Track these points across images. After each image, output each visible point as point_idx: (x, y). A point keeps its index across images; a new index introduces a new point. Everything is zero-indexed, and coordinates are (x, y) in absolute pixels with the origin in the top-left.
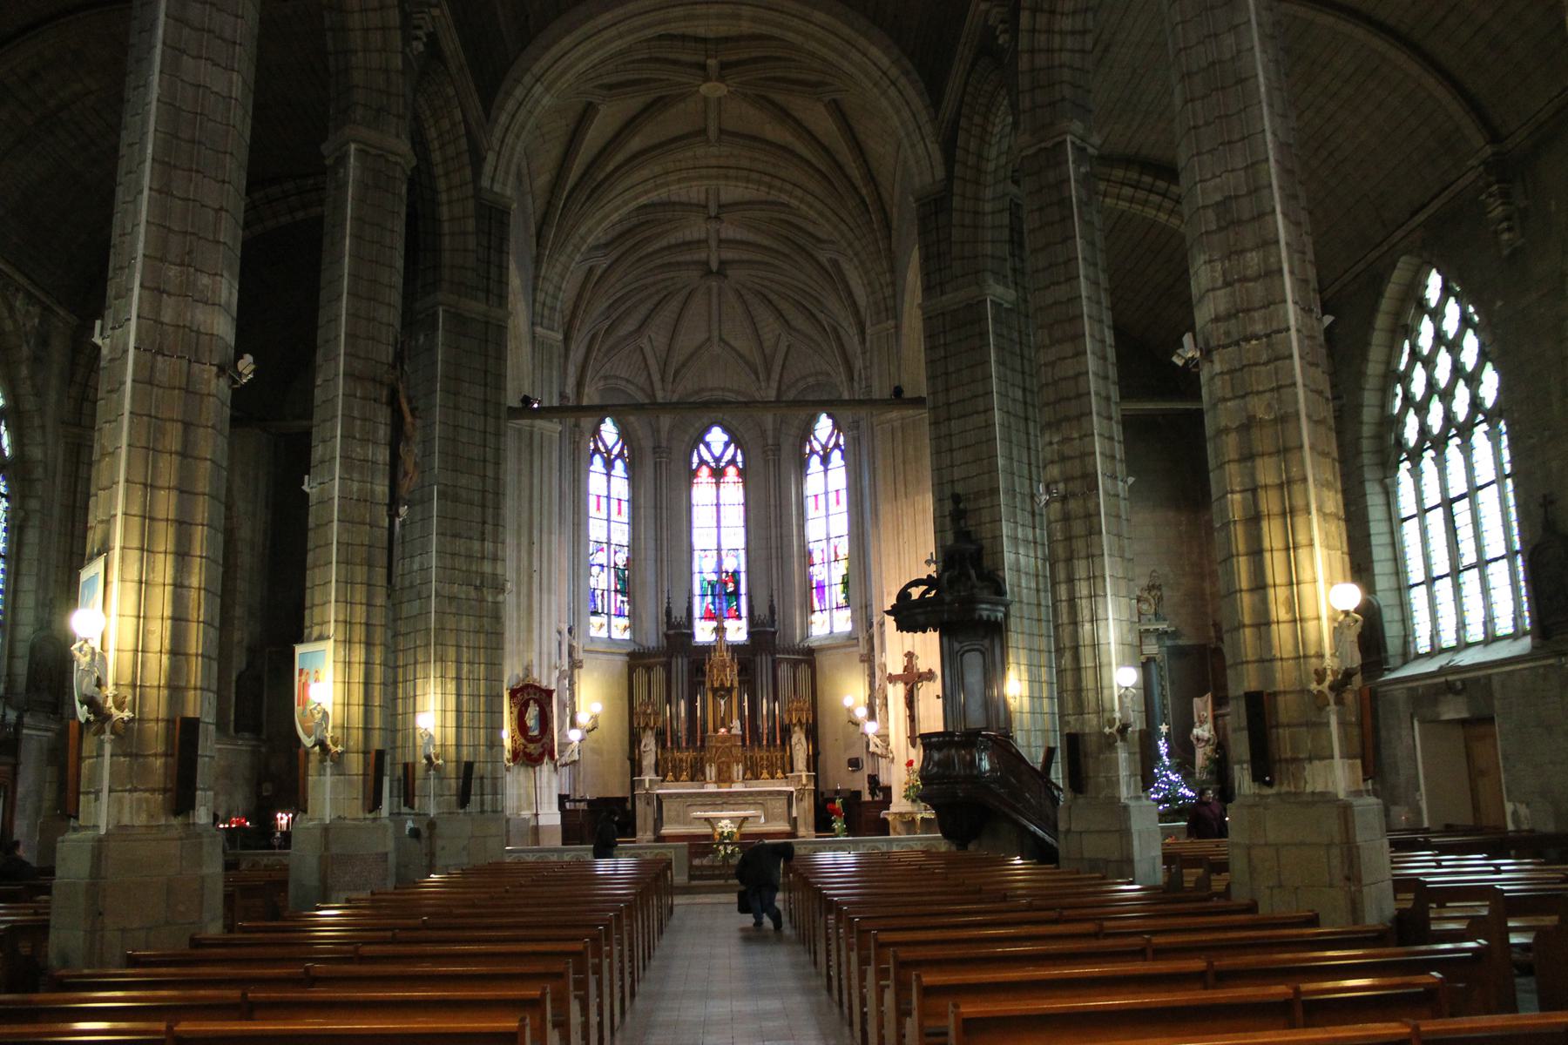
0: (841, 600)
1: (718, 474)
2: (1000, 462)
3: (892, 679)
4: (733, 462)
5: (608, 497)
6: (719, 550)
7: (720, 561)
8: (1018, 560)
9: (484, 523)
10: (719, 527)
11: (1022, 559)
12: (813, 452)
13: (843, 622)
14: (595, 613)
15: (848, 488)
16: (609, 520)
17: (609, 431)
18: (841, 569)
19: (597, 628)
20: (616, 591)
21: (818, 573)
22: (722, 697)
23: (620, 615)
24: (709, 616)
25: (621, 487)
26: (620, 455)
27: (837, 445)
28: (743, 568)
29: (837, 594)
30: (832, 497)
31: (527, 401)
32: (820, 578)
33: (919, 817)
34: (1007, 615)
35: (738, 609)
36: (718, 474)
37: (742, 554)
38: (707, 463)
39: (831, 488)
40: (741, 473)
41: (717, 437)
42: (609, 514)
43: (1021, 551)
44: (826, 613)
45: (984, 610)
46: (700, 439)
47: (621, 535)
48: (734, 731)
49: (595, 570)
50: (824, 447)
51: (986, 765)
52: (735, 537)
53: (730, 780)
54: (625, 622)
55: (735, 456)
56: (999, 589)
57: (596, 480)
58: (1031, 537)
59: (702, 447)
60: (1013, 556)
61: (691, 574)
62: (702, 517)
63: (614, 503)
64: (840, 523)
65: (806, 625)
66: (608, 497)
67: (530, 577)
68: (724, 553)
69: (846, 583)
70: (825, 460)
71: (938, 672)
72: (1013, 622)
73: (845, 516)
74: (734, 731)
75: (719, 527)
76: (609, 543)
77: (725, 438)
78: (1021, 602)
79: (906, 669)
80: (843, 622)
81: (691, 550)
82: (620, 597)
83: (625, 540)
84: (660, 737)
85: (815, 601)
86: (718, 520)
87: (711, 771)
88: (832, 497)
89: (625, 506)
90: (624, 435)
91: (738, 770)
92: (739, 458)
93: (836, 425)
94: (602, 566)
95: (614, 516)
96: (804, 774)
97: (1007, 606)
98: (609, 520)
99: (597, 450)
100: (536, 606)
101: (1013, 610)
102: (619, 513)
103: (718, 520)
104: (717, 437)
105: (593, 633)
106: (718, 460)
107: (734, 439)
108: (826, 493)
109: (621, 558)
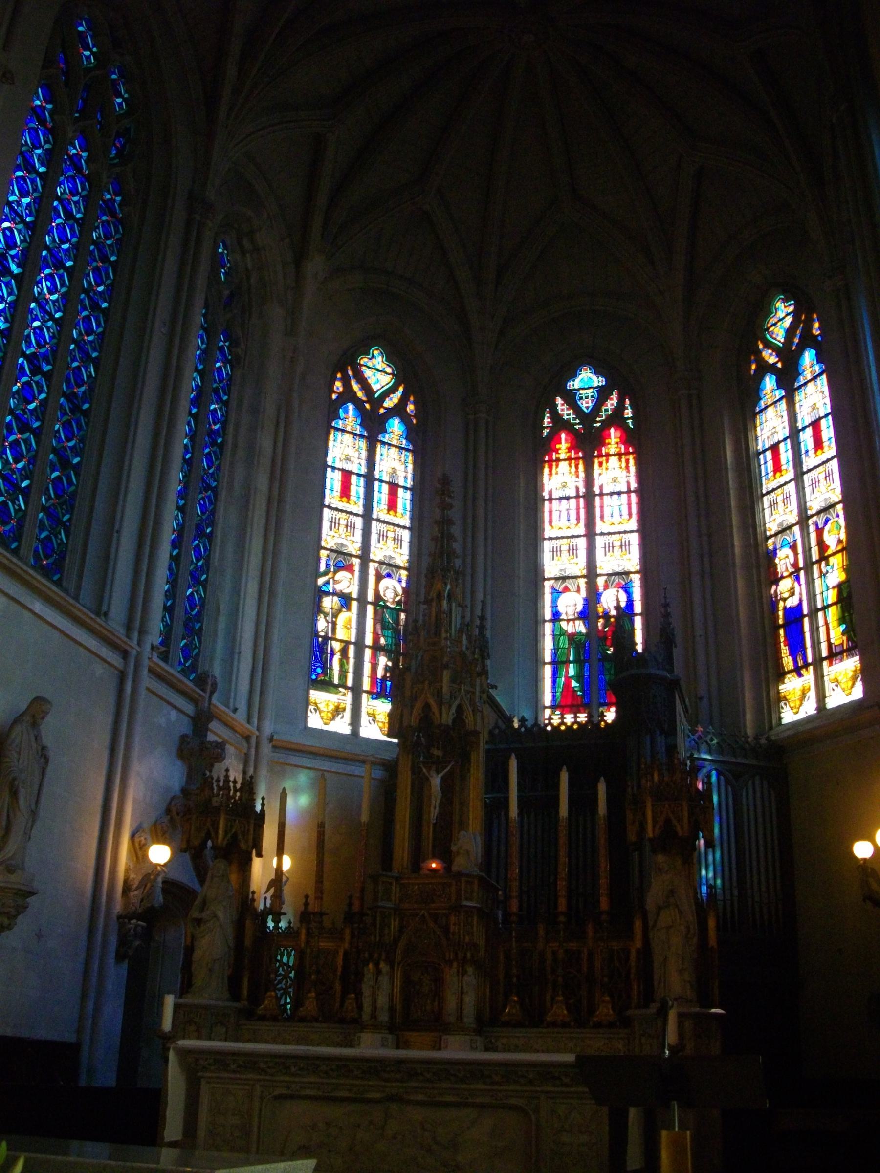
0: (837, 634)
1: (589, 446)
4: (616, 418)
5: (370, 479)
6: (591, 574)
7: (593, 597)
10: (590, 534)
12: (765, 368)
14: (326, 685)
15: (836, 413)
16: (367, 516)
17: (378, 372)
19: (325, 713)
20: (376, 648)
21: (789, 592)
22: (439, 765)
25: (395, 463)
26: (398, 411)
28: (638, 608)
30: (807, 437)
32: (792, 602)
36: (589, 446)
37: (636, 579)
38: (567, 426)
39: (804, 417)
41: (586, 381)
44: (809, 675)
46: (557, 384)
47: (394, 547)
48: (460, 864)
49: (328, 603)
52: (623, 555)
53: (438, 1026)
54: (383, 707)
57: (344, 449)
59: (559, 401)
61: (537, 622)
62: (560, 521)
63: (381, 494)
64: (826, 488)
65: (772, 702)
66: (370, 479)
68: (601, 581)
69: (846, 596)
70: (789, 380)
73: (834, 465)
74: (460, 864)
75: (590, 534)
76: (365, 556)
77: (598, 381)
81: (536, 577)
82: (383, 661)
83: (402, 557)
85: (785, 650)
86: (590, 531)
87: (381, 990)
88: (807, 437)
89: (404, 498)
90: (404, 375)
91: (463, 991)
92: (628, 413)
94: (346, 599)
95: (380, 509)
98: (367, 516)
99: (348, 395)
102: (392, 505)
103: (590, 531)
104: (586, 381)
105: (314, 721)
106: (587, 418)
107: (616, 379)
108: (794, 434)
109: (392, 589)
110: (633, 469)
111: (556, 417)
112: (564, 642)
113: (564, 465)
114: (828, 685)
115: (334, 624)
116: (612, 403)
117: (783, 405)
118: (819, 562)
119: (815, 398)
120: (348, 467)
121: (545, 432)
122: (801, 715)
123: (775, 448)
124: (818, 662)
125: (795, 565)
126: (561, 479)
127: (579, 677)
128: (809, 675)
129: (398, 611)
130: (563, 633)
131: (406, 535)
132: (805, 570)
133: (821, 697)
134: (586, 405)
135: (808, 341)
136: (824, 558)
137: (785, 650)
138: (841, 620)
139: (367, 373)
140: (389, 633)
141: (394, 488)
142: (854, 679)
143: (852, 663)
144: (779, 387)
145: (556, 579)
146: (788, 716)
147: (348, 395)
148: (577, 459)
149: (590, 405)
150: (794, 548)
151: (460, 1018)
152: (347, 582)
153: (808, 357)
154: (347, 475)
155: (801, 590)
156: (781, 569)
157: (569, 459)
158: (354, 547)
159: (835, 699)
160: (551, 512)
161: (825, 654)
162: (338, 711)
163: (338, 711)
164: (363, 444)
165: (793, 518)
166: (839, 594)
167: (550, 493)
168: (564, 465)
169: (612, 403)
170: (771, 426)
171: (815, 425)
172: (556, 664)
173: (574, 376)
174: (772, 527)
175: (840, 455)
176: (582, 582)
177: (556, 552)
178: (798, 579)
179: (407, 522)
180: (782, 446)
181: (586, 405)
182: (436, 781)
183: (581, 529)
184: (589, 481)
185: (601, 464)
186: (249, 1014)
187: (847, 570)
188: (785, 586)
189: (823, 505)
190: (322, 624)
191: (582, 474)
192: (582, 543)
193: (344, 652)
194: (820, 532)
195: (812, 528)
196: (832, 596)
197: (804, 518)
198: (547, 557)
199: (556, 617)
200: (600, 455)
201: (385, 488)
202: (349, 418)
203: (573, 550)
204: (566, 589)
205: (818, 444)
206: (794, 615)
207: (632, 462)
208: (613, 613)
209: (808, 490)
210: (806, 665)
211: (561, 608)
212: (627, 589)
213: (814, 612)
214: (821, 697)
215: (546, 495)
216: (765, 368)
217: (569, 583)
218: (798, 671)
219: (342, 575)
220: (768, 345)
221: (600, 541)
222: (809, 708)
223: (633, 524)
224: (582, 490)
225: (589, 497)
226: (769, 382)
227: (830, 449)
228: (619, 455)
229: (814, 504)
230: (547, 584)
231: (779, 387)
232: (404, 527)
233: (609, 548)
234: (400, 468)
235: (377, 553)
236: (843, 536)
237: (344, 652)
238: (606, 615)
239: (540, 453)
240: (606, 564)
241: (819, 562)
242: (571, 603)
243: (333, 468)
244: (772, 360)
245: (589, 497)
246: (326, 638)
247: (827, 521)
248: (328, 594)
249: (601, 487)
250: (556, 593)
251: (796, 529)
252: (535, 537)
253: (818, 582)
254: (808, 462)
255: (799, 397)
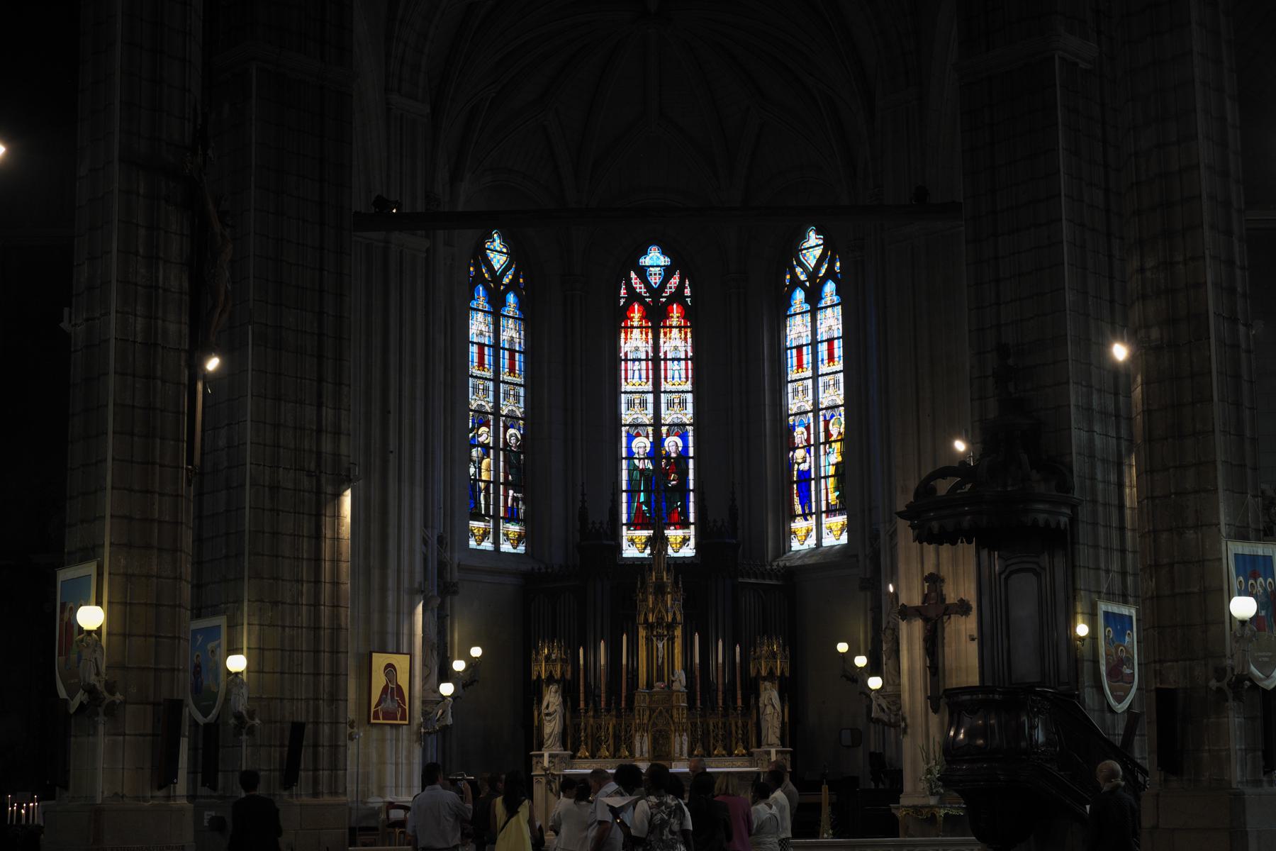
0: (833, 497)
2: (1069, 297)
3: (906, 613)
4: (678, 296)
6: (657, 422)
7: (658, 442)
8: (1091, 441)
9: (320, 380)
10: (657, 392)
11: (1098, 440)
12: (796, 283)
13: (835, 532)
14: (478, 517)
15: (845, 337)
16: (496, 380)
18: (835, 458)
22: (660, 637)
23: (512, 517)
24: (637, 522)
25: (511, 332)
26: (512, 286)
27: (830, 274)
29: (829, 492)
30: (823, 348)
31: (382, 204)
32: (804, 467)
33: (942, 812)
34: (1073, 520)
35: (685, 512)
39: (823, 334)
40: (687, 314)
41: (655, 259)
42: (497, 372)
43: (1097, 428)
44: (812, 521)
45: (1041, 514)
49: (475, 453)
50: (812, 275)
51: (1040, 736)
54: (514, 528)
55: (681, 287)
56: (1065, 486)
57: (478, 325)
58: (1111, 408)
59: (633, 275)
60: (1084, 435)
61: (617, 460)
62: (634, 379)
65: (785, 535)
66: (496, 347)
67: (385, 462)
68: (664, 430)
70: (814, 297)
71: (974, 605)
72: (1083, 531)
75: (657, 392)
77: (664, 261)
78: (1094, 502)
79: (926, 598)
80: (835, 532)
81: (617, 422)
82: (511, 492)
84: (569, 692)
85: (796, 500)
88: (823, 348)
92: (688, 292)
93: (827, 245)
94: (485, 447)
96: (773, 751)
97: (1074, 507)
98: (496, 380)
99: (479, 278)
100: (392, 502)
101: (1084, 513)
104: (655, 259)
105: (472, 543)
106: (656, 292)
108: (814, 343)
110: (689, 341)
111: (630, 289)
112: (636, 475)
113: (636, 332)
114: (825, 531)
115: (480, 469)
116: (675, 281)
117: (808, 317)
118: (825, 444)
119: (831, 322)
120: (482, 340)
121: (622, 301)
122: (805, 547)
123: (799, 348)
124: (819, 514)
125: (808, 440)
126: (634, 343)
127: (647, 503)
128: (812, 521)
129: (518, 454)
130: (636, 468)
131: (522, 391)
132: (812, 446)
133: (819, 538)
134: (655, 281)
135: (830, 274)
136: (828, 442)
137: (796, 500)
138: (836, 489)
139: (491, 255)
140: (514, 471)
141: (512, 352)
142: (842, 530)
143: (841, 520)
144: (806, 301)
145: (630, 425)
146: (796, 545)
147: (479, 278)
148: (647, 327)
149: (658, 281)
150: (808, 428)
151: (681, 754)
152: (485, 435)
153: (830, 287)
154: (481, 346)
155: (811, 459)
156: (797, 440)
157: (641, 327)
158: (488, 408)
159: (828, 541)
160: (626, 370)
161: (824, 509)
162: (485, 535)
163: (485, 535)
164: (490, 319)
165: (808, 407)
166: (836, 470)
167: (626, 354)
168: (636, 332)
169: (675, 281)
170: (797, 330)
171: (830, 341)
172: (632, 492)
173: (645, 253)
174: (793, 408)
175: (845, 371)
176: (650, 429)
177: (631, 404)
178: (809, 451)
179: (521, 380)
180: (805, 349)
181: (655, 281)
182: (660, 646)
183: (649, 387)
184: (656, 347)
185: (665, 334)
186: (573, 757)
187: (842, 454)
188: (800, 454)
189: (831, 404)
190: (472, 470)
191: (651, 341)
192: (650, 398)
193: (487, 489)
194: (827, 423)
195: (821, 418)
196: (832, 470)
197: (816, 410)
198: (624, 407)
199: (631, 456)
200: (665, 327)
201: (507, 353)
202: (481, 300)
203: (643, 404)
204: (638, 435)
205: (831, 358)
206: (805, 477)
207: (689, 335)
208: (673, 455)
209: (821, 389)
210: (811, 514)
211: (635, 450)
212: (684, 437)
213: (818, 479)
214: (819, 538)
215: (622, 355)
216: (796, 283)
217: (640, 430)
218: (805, 516)
219: (483, 429)
220: (801, 264)
221: (663, 397)
222: (811, 542)
223: (688, 386)
224: (651, 354)
225: (656, 360)
226: (799, 295)
227: (839, 366)
228: (680, 327)
229: (824, 402)
230: (624, 429)
231: (806, 301)
232: (520, 385)
233: (670, 404)
234: (515, 335)
235: (505, 411)
236: (842, 430)
237: (487, 489)
238: (668, 456)
239: (616, 322)
240: (668, 416)
241: (825, 444)
242: (642, 444)
243: (473, 343)
244: (803, 277)
245: (656, 360)
246: (475, 480)
247: (832, 416)
248: (475, 446)
249: (665, 353)
250: (630, 438)
251: (810, 415)
252: (616, 392)
253: (822, 458)
254: (823, 369)
255: (820, 316)
